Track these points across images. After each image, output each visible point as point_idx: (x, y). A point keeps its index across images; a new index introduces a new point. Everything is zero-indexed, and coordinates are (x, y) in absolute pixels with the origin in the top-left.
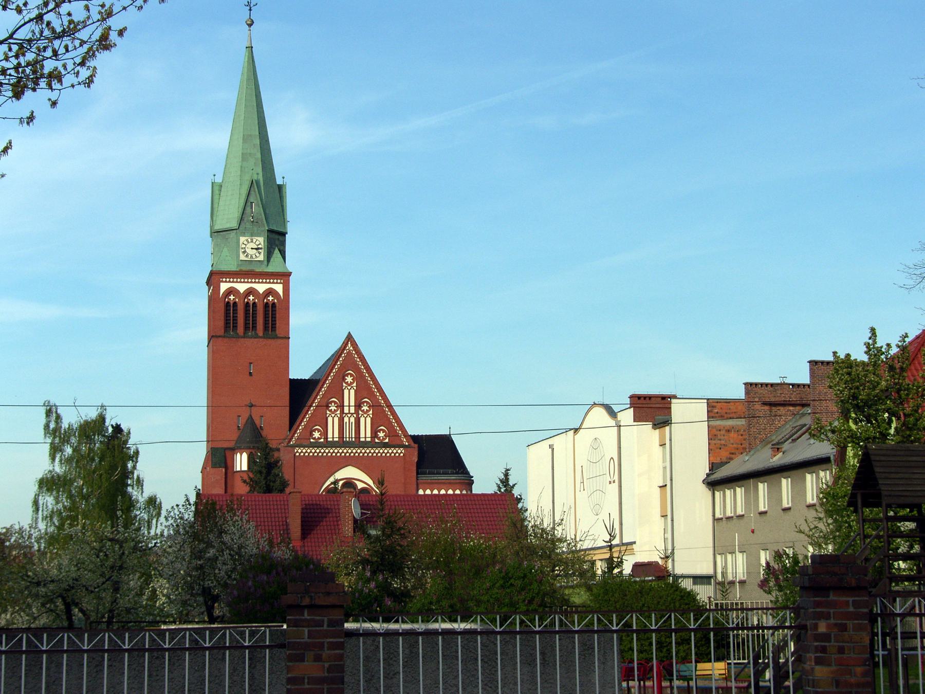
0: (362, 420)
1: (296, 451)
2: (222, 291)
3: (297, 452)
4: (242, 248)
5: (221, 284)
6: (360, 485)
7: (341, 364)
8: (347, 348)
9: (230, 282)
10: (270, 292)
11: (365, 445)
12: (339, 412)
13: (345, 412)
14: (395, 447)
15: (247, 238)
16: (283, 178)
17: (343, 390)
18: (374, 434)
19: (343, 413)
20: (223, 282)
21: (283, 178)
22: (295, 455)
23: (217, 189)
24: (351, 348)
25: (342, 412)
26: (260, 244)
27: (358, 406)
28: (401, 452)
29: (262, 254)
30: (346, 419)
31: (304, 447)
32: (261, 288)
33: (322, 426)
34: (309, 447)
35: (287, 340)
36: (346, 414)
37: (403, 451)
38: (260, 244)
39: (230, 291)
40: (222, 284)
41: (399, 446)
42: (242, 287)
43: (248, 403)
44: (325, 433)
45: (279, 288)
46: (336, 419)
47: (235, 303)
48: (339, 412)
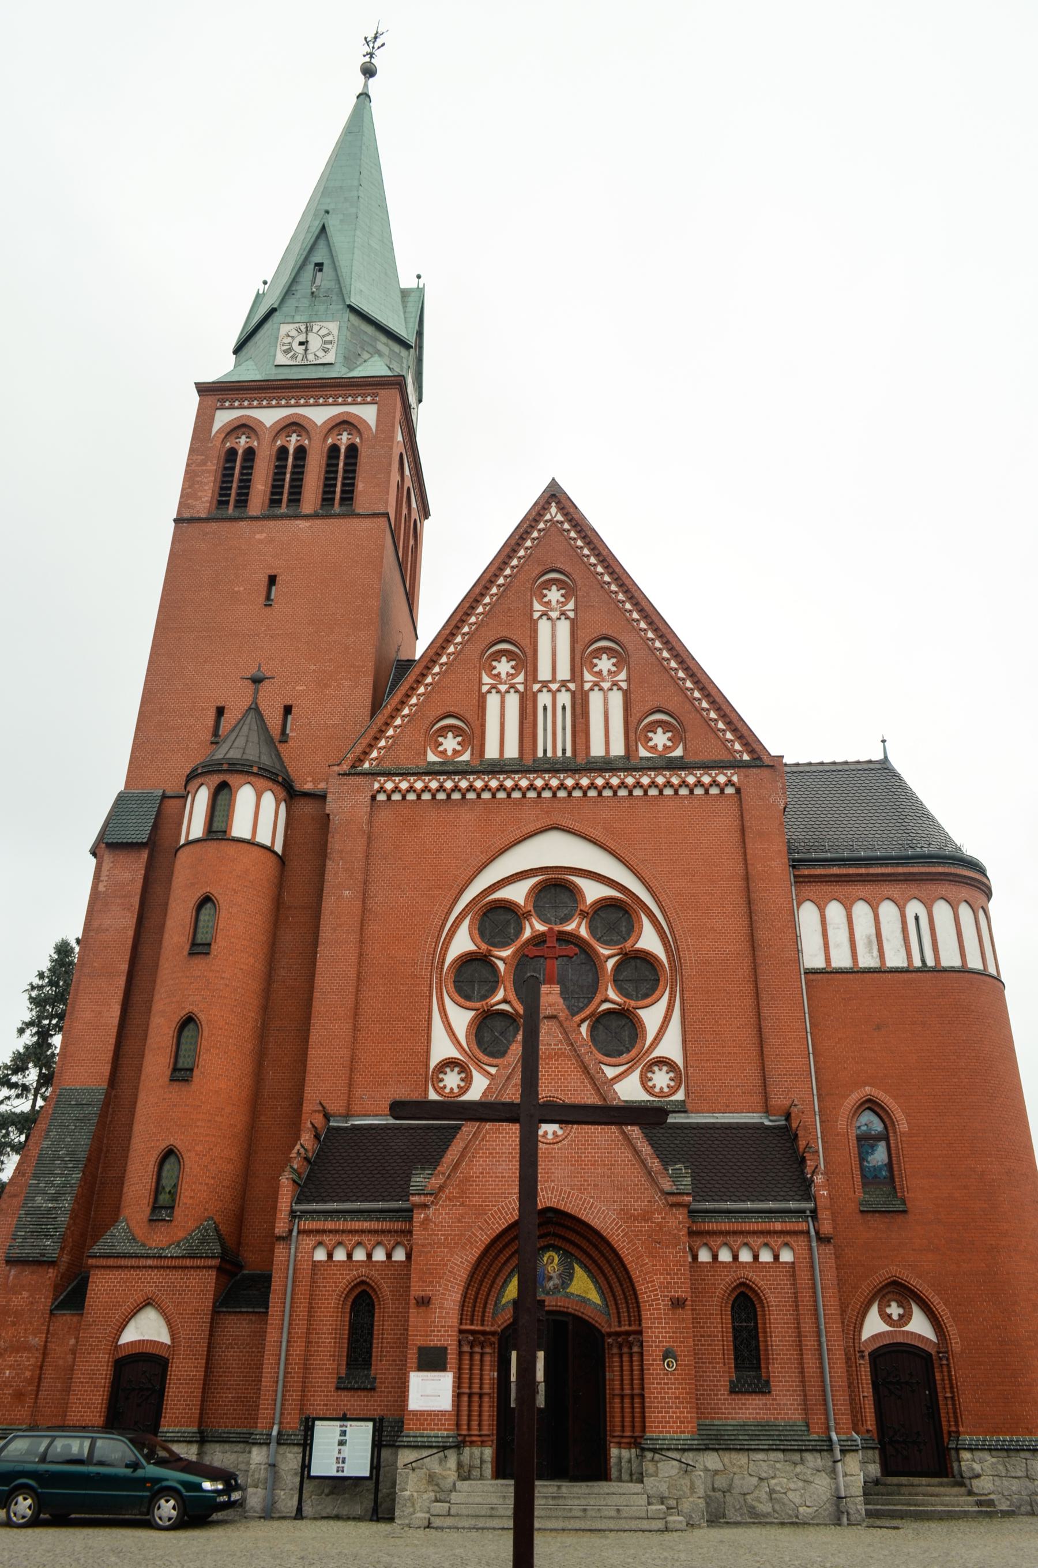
0: (595, 700)
1: (376, 786)
2: (217, 426)
3: (381, 789)
4: (284, 344)
6: (593, 892)
8: (548, 517)
10: (344, 424)
11: (606, 765)
12: (520, 678)
13: (540, 679)
14: (706, 767)
15: (297, 325)
16: (419, 277)
17: (535, 623)
18: (633, 733)
19: (535, 681)
21: (419, 277)
22: (373, 798)
24: (559, 517)
26: (329, 334)
27: (580, 660)
28: (730, 783)
30: (544, 699)
31: (405, 775)
32: (319, 415)
33: (468, 716)
34: (418, 774)
36: (545, 684)
37: (735, 779)
38: (329, 334)
39: (243, 427)
41: (721, 766)
42: (269, 417)
43: (252, 671)
44: (474, 737)
45: (368, 413)
46: (513, 701)
48: (520, 678)
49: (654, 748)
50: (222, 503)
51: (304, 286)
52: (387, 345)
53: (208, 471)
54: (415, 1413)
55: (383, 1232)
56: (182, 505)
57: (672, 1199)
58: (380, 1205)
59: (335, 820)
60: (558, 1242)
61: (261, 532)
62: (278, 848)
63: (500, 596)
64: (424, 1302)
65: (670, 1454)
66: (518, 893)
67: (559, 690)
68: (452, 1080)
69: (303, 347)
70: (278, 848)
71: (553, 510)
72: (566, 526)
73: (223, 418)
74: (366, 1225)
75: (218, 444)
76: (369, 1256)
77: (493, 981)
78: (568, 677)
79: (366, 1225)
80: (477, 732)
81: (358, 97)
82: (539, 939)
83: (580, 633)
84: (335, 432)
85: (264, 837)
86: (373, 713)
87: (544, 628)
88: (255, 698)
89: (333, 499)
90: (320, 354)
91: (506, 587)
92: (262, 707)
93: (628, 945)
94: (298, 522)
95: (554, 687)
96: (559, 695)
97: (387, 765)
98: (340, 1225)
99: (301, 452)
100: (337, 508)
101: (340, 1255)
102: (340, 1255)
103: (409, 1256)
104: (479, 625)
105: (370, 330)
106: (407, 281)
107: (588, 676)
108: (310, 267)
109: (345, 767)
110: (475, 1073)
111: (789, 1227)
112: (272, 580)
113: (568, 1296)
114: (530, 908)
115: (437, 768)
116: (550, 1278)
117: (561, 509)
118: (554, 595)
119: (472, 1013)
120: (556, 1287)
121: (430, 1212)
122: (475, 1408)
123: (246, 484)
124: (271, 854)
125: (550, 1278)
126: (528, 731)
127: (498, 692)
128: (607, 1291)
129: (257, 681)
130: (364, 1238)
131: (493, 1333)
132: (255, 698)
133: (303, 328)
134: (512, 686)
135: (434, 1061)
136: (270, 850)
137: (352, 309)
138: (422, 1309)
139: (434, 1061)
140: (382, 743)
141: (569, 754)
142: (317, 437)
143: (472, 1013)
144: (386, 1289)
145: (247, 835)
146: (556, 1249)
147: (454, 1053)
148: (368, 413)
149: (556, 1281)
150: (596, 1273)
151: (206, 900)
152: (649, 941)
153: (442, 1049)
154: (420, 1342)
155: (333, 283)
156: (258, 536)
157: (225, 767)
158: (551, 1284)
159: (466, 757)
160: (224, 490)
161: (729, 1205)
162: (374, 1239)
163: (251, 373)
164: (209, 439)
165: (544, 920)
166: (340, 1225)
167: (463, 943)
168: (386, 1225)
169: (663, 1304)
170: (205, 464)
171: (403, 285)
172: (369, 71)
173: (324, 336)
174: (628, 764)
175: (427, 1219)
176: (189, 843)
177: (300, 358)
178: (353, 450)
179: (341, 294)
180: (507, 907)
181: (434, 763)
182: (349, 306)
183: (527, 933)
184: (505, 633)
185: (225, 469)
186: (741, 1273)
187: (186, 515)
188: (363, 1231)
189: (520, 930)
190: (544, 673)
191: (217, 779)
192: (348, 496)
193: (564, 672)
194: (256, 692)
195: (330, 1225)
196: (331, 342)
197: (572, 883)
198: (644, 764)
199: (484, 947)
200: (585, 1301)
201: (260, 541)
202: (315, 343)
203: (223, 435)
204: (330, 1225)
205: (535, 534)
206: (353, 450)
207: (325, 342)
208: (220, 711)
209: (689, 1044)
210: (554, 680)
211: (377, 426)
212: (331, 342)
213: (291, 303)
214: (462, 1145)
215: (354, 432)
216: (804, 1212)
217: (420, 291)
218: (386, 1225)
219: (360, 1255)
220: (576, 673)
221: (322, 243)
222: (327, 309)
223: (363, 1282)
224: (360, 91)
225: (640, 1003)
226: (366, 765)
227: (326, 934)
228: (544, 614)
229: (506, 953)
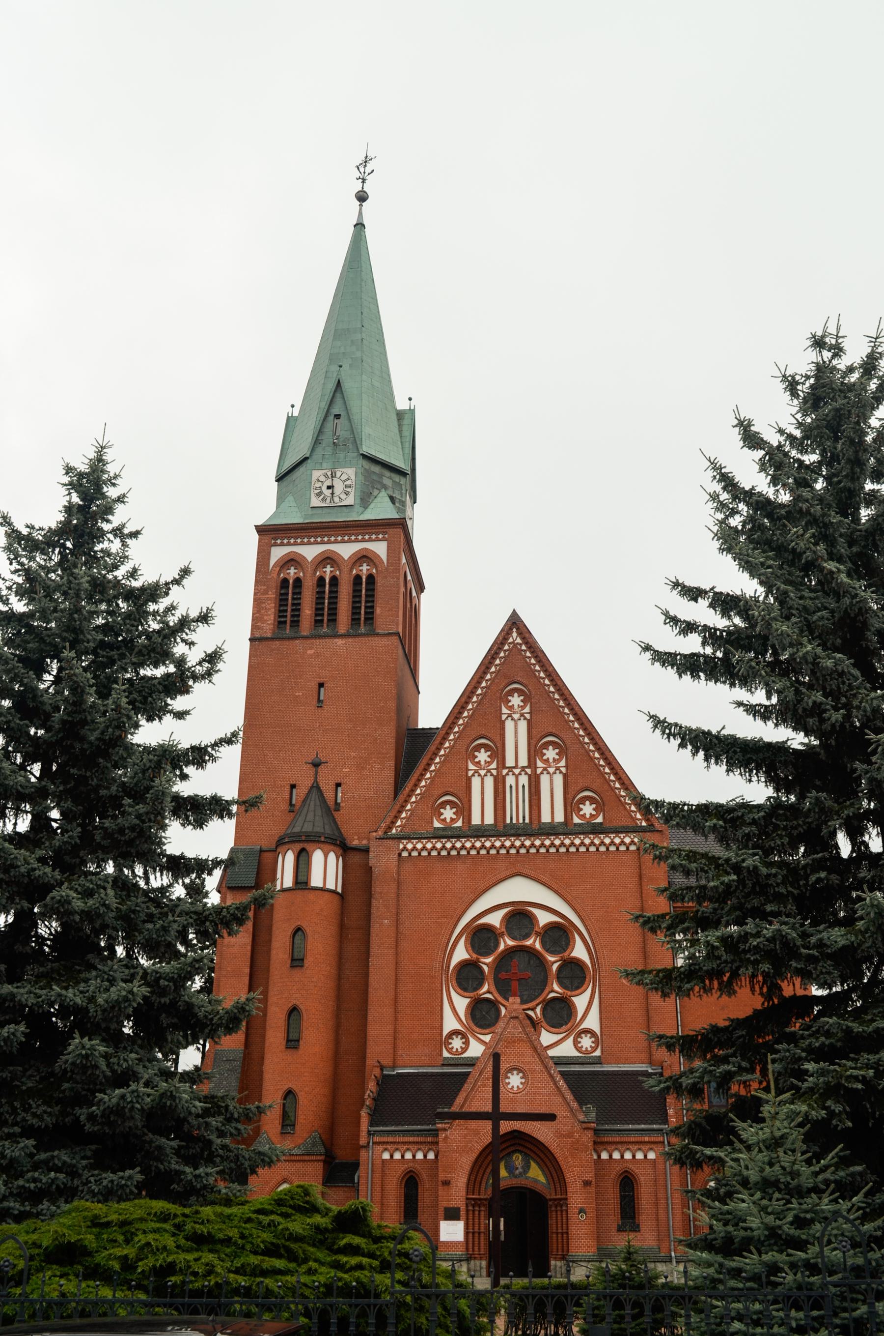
0: (545, 780)
1: (401, 846)
2: (273, 561)
3: (405, 848)
6: (544, 918)
7: (497, 673)
8: (511, 640)
10: (364, 557)
11: (552, 830)
12: (494, 765)
13: (507, 765)
14: (617, 832)
15: (325, 471)
16: (410, 399)
17: (503, 723)
18: (571, 806)
19: (504, 767)
20: (276, 545)
21: (410, 399)
22: (400, 855)
23: (291, 421)
24: (519, 641)
25: (502, 764)
26: (348, 479)
27: (535, 752)
28: (632, 842)
29: (352, 495)
30: (510, 780)
32: (346, 550)
33: (460, 794)
34: (429, 838)
36: (511, 769)
37: (636, 840)
38: (348, 479)
39: (291, 561)
40: (274, 549)
41: (627, 830)
42: (310, 552)
43: (312, 757)
44: (464, 810)
45: (380, 549)
46: (489, 782)
48: (494, 765)
49: (584, 816)
50: (281, 624)
51: (327, 438)
52: (390, 478)
53: (270, 599)
54: (444, 1243)
55: (421, 1143)
56: (254, 627)
57: (584, 1125)
58: (419, 1127)
59: (376, 870)
60: (521, 1148)
61: (311, 648)
62: (339, 890)
63: (479, 703)
64: (447, 1183)
65: (581, 1263)
66: (495, 919)
67: (520, 774)
68: (457, 1043)
69: (330, 491)
70: (339, 890)
71: (515, 635)
72: (524, 647)
73: (277, 553)
74: (411, 1139)
75: (275, 576)
76: (414, 1156)
77: (480, 979)
78: (526, 764)
79: (411, 1139)
80: (466, 806)
81: (355, 226)
82: (510, 952)
83: (534, 731)
84: (358, 564)
85: (331, 885)
86: (396, 794)
87: (509, 725)
88: (316, 778)
89: (360, 619)
90: (343, 496)
91: (484, 695)
92: (321, 785)
93: (566, 954)
94: (336, 640)
95: (517, 771)
96: (520, 777)
97: (407, 830)
98: (397, 1139)
99: (334, 580)
100: (363, 629)
101: (397, 1156)
102: (397, 1156)
103: (436, 1156)
104: (466, 725)
106: (401, 404)
107: (539, 764)
108: (331, 418)
109: (380, 833)
111: (653, 1139)
112: (321, 685)
113: (527, 1178)
114: (504, 930)
115: (441, 833)
116: (517, 1168)
117: (520, 634)
118: (516, 700)
119: (468, 1000)
120: (520, 1173)
121: (448, 1132)
122: (476, 1240)
123: (297, 609)
124: (335, 895)
125: (517, 1168)
126: (500, 806)
127: (479, 775)
128: (549, 1175)
129: (316, 765)
130: (410, 1146)
131: (485, 1199)
132: (316, 778)
133: (329, 473)
135: (446, 1032)
137: (365, 457)
138: (446, 1187)
139: (445, 1032)
140: (404, 815)
141: (527, 821)
142: (345, 570)
143: (468, 1000)
144: (424, 1175)
145: (320, 885)
146: (520, 1152)
147: (458, 1027)
148: (380, 549)
149: (521, 1170)
150: (542, 1165)
151: (298, 929)
152: (579, 952)
153: (450, 1024)
154: (445, 1204)
155: (349, 433)
156: (309, 652)
157: (303, 838)
158: (517, 1172)
159: (459, 824)
160: (281, 613)
161: (619, 1127)
162: (416, 1147)
163: (295, 517)
164: (267, 572)
165: (513, 938)
166: (397, 1139)
167: (461, 954)
168: (423, 1139)
169: (579, 1184)
170: (267, 593)
171: (399, 407)
172: (362, 197)
173: (345, 481)
174: (565, 829)
175: (446, 1137)
176: (283, 890)
177: (328, 500)
178: (371, 578)
180: (488, 929)
181: (438, 829)
182: (362, 455)
183: (502, 947)
184: (483, 732)
185: (281, 594)
186: (626, 1165)
187: (257, 635)
188: (410, 1143)
189: (497, 945)
190: (510, 762)
191: (298, 846)
192: (370, 618)
193: (523, 761)
194: (316, 773)
195: (391, 1139)
196: (350, 486)
197: (530, 912)
198: (577, 829)
199: (475, 956)
200: (536, 1181)
201: (311, 656)
202: (339, 488)
203: (278, 569)
204: (391, 1139)
205: (502, 654)
207: (346, 486)
208: (293, 786)
209: (604, 1021)
210: (516, 767)
211: (388, 560)
212: (350, 486)
213: (319, 451)
214: (465, 1094)
215: (371, 564)
216: (662, 1130)
217: (412, 412)
218: (423, 1139)
219: (408, 1156)
220: (532, 763)
221: (338, 395)
222: (345, 457)
223: (411, 1171)
224: (355, 223)
225: (574, 993)
226: (394, 831)
227: (374, 950)
228: (509, 716)
229: (489, 960)
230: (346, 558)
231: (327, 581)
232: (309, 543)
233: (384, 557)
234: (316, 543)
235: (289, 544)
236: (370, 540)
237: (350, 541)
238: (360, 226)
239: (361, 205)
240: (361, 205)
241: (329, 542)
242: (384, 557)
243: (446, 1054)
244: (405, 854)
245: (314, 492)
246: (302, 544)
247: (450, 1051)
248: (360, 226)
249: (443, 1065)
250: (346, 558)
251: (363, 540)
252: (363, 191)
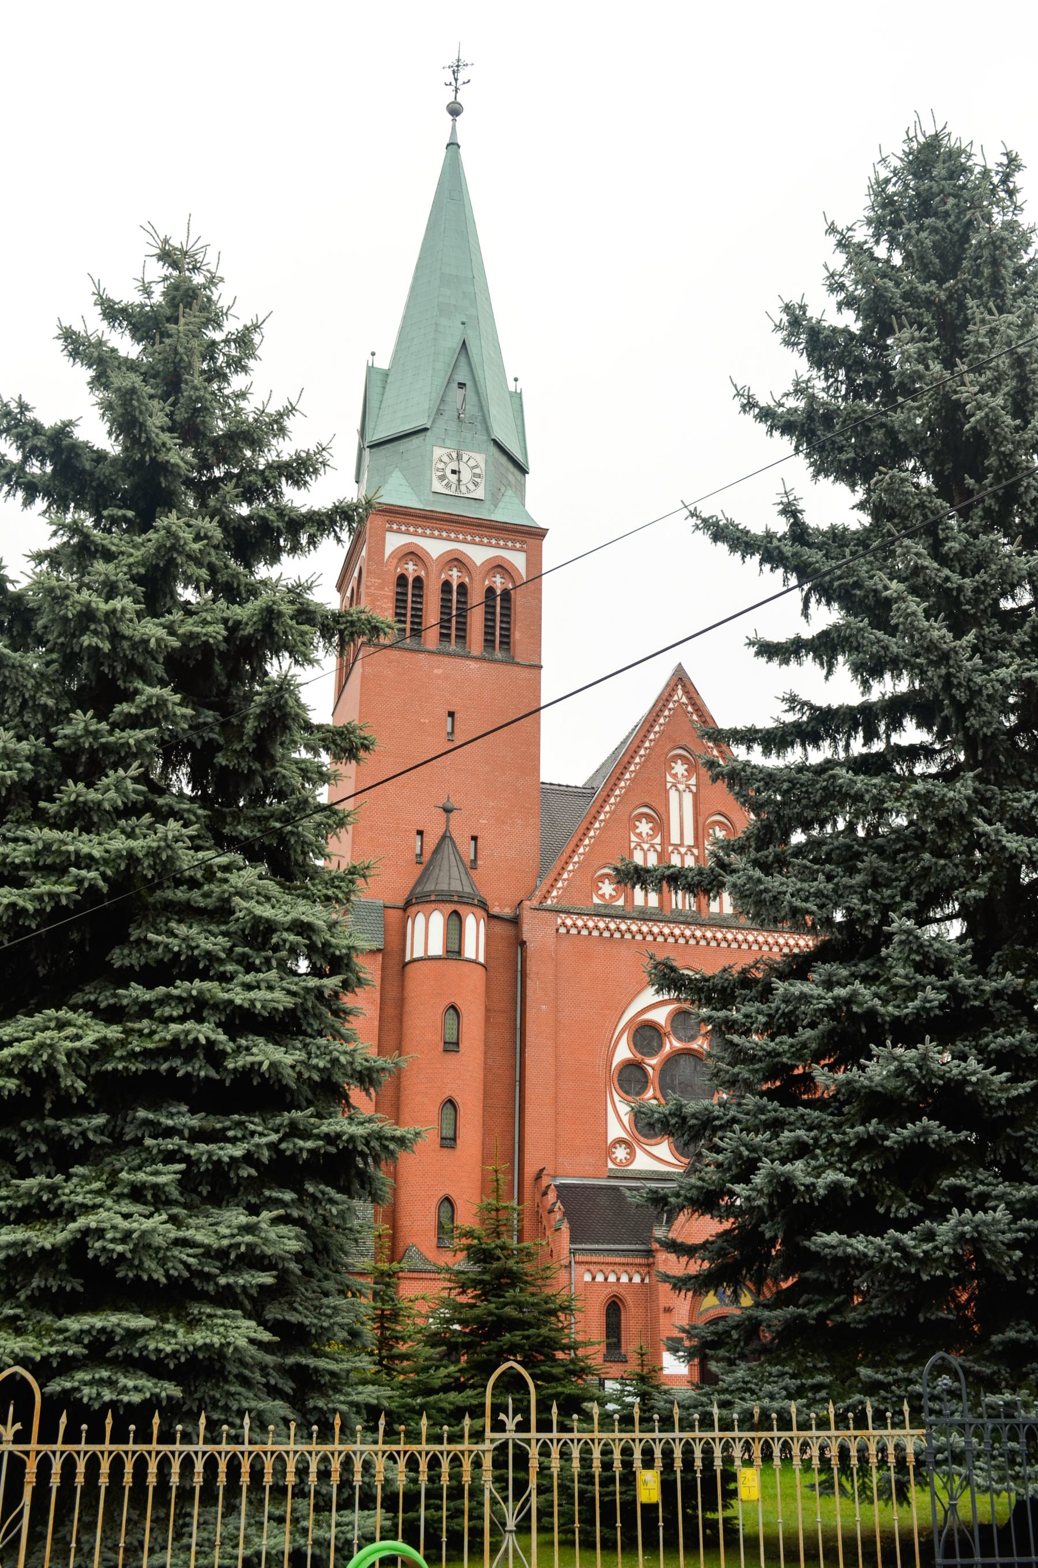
1: (559, 921)
4: (438, 470)
5: (389, 535)
7: (661, 733)
8: (676, 698)
9: (407, 532)
13: (673, 841)
17: (667, 792)
20: (391, 530)
24: (684, 700)
25: (666, 840)
26: (477, 466)
29: (482, 487)
32: (479, 554)
35: (536, 671)
38: (477, 466)
42: (435, 548)
45: (518, 560)
47: (418, 580)
48: (658, 840)
53: (386, 597)
58: (625, 1247)
59: (531, 946)
61: (438, 667)
63: (643, 765)
64: (668, 1310)
68: (621, 1153)
69: (456, 477)
71: (680, 692)
72: (690, 709)
74: (618, 1260)
75: (392, 569)
77: (644, 1083)
78: (692, 843)
79: (618, 1260)
82: (677, 1055)
83: (702, 807)
87: (673, 795)
88: (447, 826)
90: (472, 487)
91: (647, 757)
94: (468, 662)
95: (683, 850)
97: (564, 904)
101: (600, 1278)
102: (600, 1278)
104: (628, 789)
105: (504, 460)
108: (455, 385)
109: (535, 903)
110: (638, 1150)
115: (603, 911)
117: (686, 692)
118: (680, 768)
123: (418, 615)
127: (642, 849)
132: (447, 826)
133: (454, 455)
134: (652, 846)
135: (610, 1139)
136: (475, 962)
139: (610, 1139)
140: (560, 884)
141: (694, 909)
142: (477, 578)
144: (629, 1300)
145: (474, 957)
147: (623, 1135)
153: (615, 1131)
155: (476, 409)
156: (436, 671)
157: (456, 899)
159: (621, 902)
164: (381, 562)
165: (679, 1039)
167: (623, 1052)
168: (630, 1260)
170: (383, 589)
172: (455, 110)
173: (473, 468)
177: (454, 487)
178: (506, 595)
179: (488, 430)
180: (651, 1027)
181: (598, 905)
182: (494, 441)
183: (667, 1048)
184: (647, 800)
185: (398, 593)
189: (661, 1046)
190: (675, 839)
191: (451, 907)
192: (506, 642)
193: (689, 840)
194: (448, 820)
195: (594, 1259)
196: (479, 476)
199: (639, 1057)
201: (438, 676)
202: (466, 475)
203: (395, 561)
204: (594, 1259)
205: (666, 713)
206: (506, 595)
207: (475, 475)
210: (682, 845)
212: (479, 476)
213: (441, 424)
215: (507, 576)
218: (630, 1260)
219: (612, 1278)
222: (473, 438)
226: (549, 902)
227: (530, 1039)
228: (674, 785)
229: (653, 1061)
230: (478, 563)
231: (455, 587)
232: (481, 544)
233: (523, 570)
234: (489, 545)
235: (497, 546)
236: (465, 541)
237: (440, 538)
238: (453, 145)
239: (454, 120)
240: (454, 120)
241: (416, 534)
242: (523, 570)
243: (611, 1165)
244: (574, 931)
245: (435, 475)
246: (473, 543)
247: (614, 1161)
248: (453, 145)
249: (609, 1177)
250: (478, 563)
251: (456, 540)
252: (455, 102)
